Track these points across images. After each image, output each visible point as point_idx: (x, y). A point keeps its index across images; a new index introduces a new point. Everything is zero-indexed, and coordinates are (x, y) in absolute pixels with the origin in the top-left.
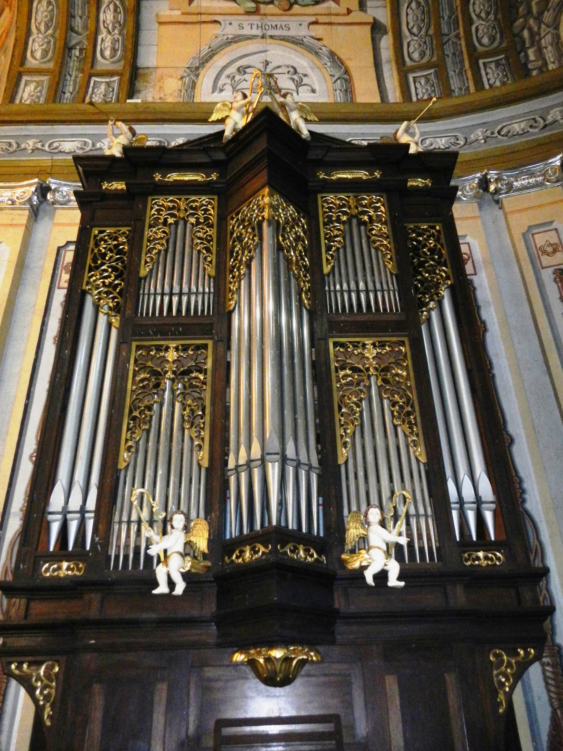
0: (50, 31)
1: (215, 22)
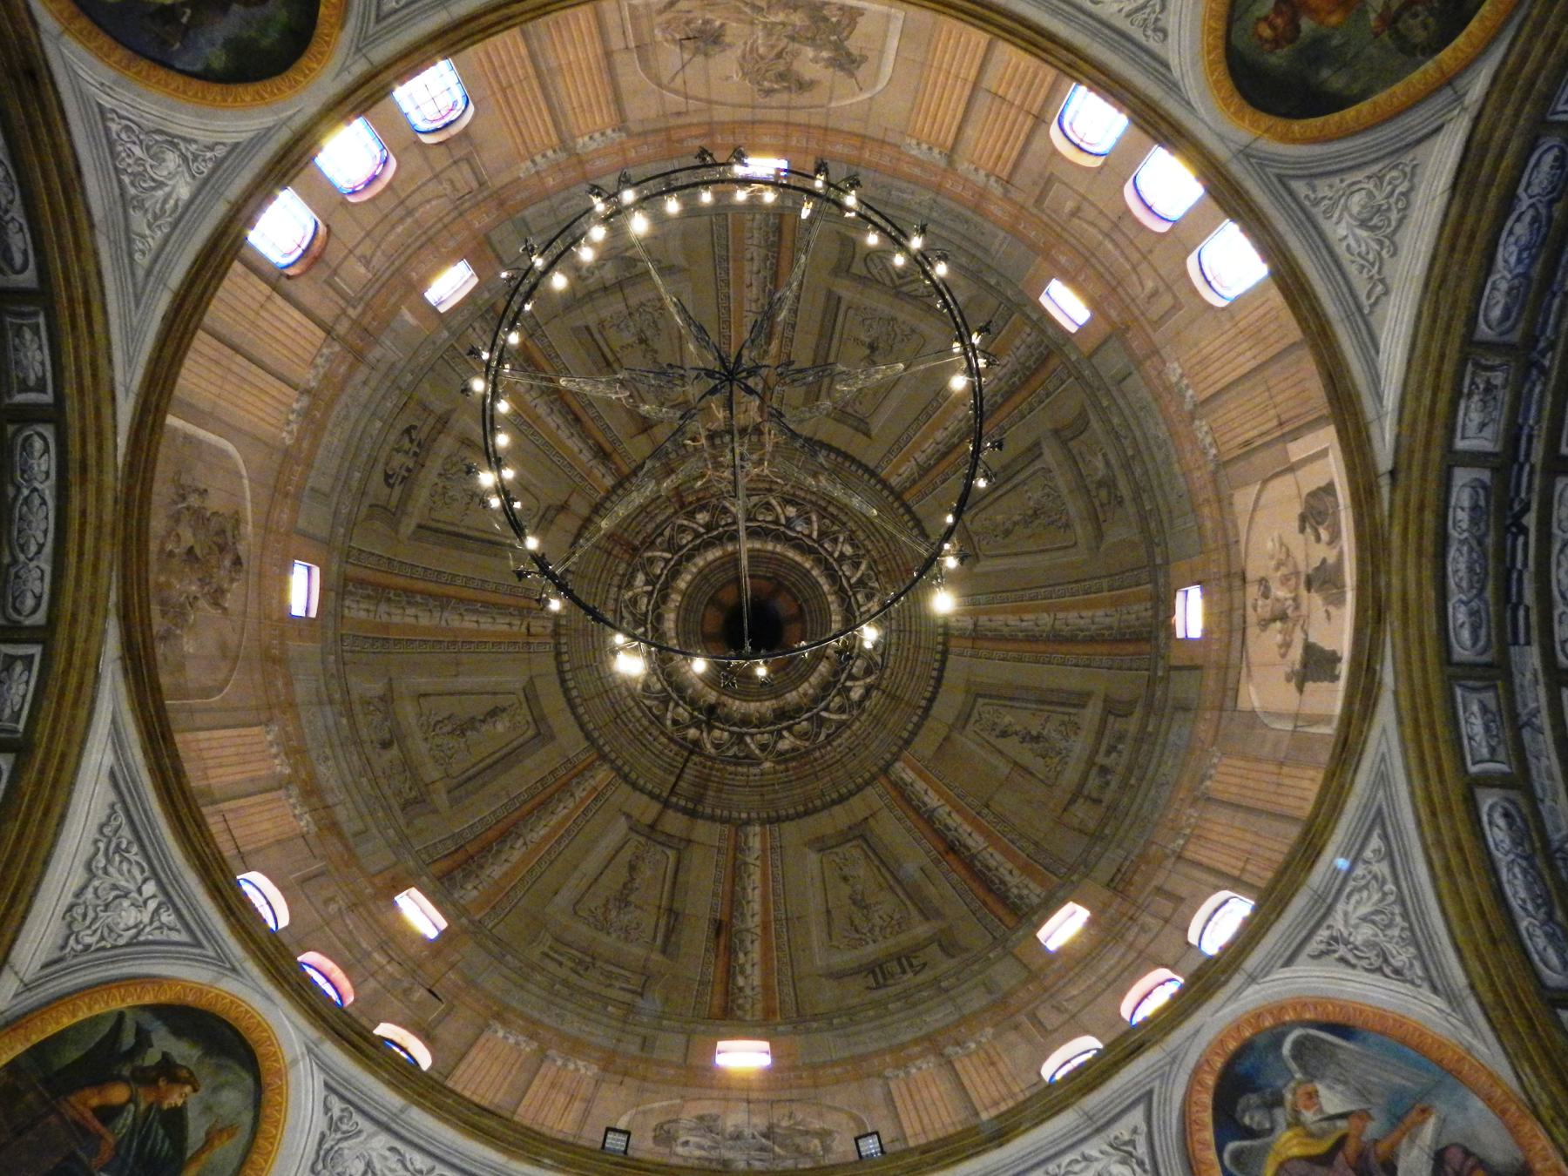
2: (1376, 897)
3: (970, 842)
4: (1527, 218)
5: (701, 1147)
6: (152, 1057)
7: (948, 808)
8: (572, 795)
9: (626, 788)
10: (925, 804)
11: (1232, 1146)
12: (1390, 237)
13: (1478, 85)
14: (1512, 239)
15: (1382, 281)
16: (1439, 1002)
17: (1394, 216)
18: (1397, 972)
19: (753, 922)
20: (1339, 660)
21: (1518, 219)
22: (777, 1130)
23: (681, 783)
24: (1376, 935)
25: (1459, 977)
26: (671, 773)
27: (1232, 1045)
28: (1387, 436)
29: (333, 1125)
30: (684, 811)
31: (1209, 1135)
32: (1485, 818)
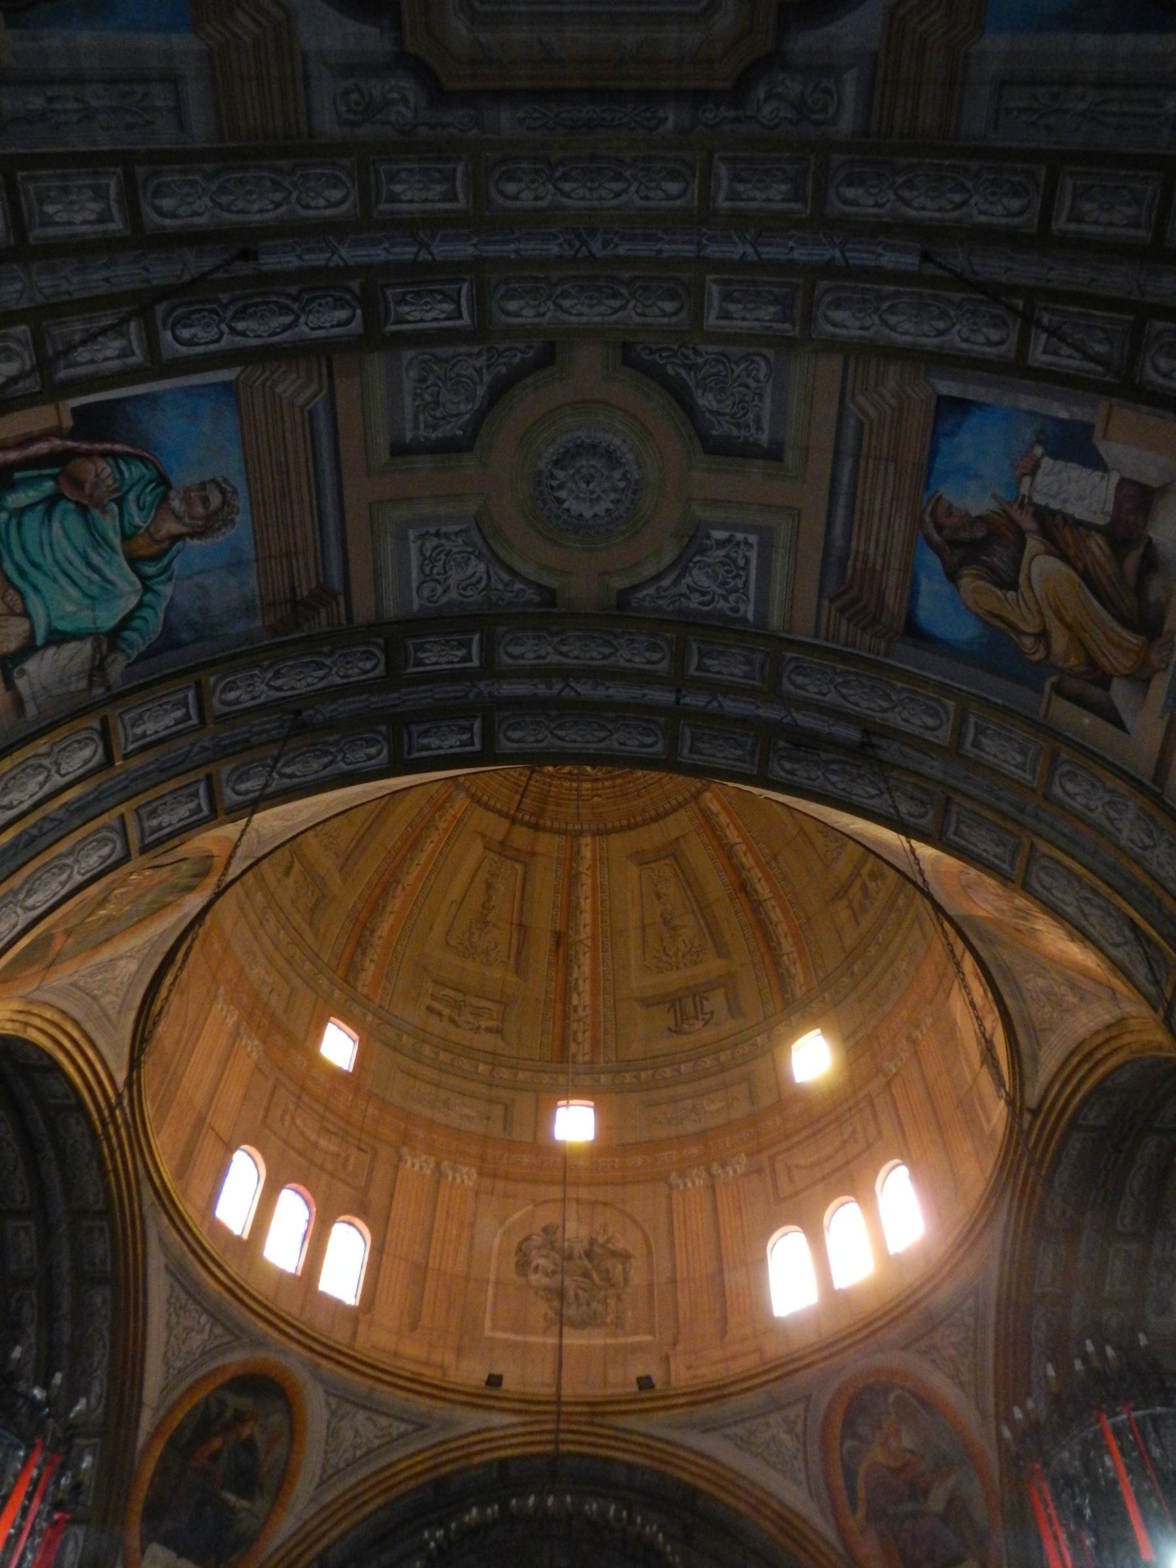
3: (758, 887)
5: (547, 1275)
6: (229, 1413)
7: (744, 848)
8: (437, 829)
9: (479, 811)
10: (726, 836)
11: (848, 1443)
19: (585, 933)
22: (595, 1248)
23: (525, 800)
26: (516, 792)
29: (333, 1413)
30: (528, 825)
31: (837, 1431)
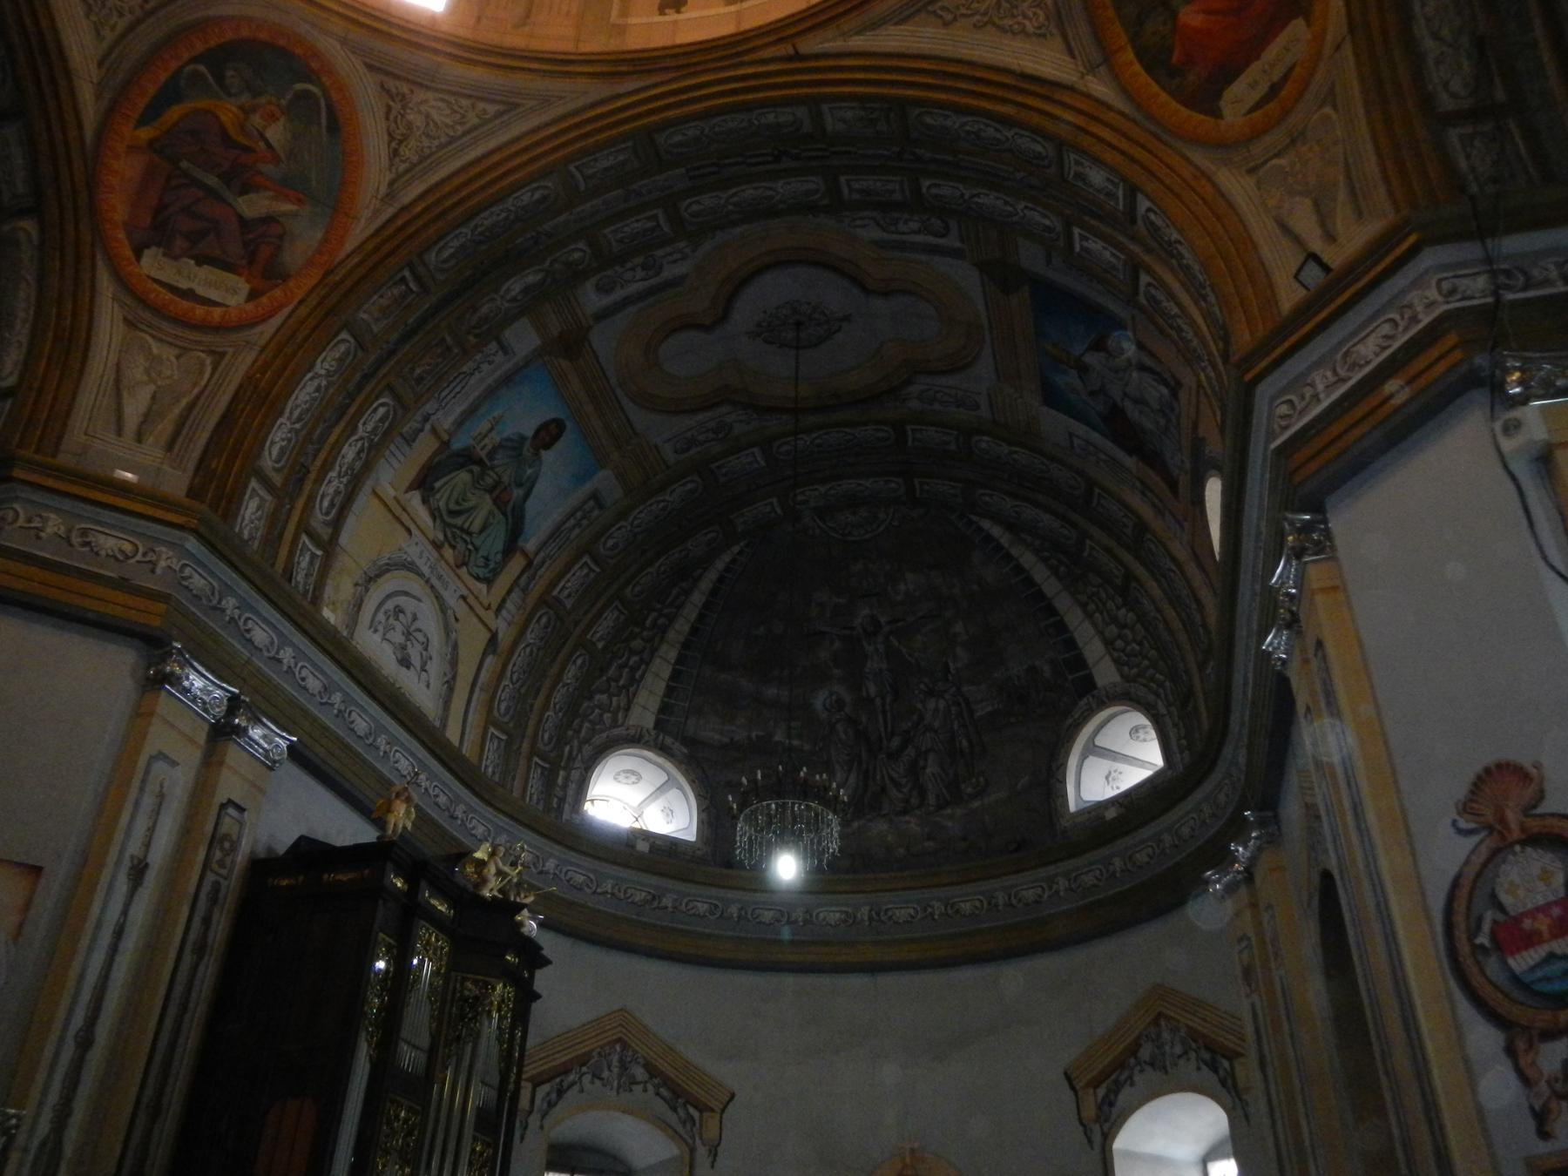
0: (297, 426)
1: (409, 531)
2: (448, 121)
4: (998, 136)
11: (202, 68)
12: (991, 22)
13: (1100, 88)
14: (982, 127)
15: (955, 19)
16: (383, 189)
17: (1008, 22)
18: (396, 153)
20: (678, 12)
21: (997, 130)
24: (418, 128)
25: (407, 199)
27: (282, 42)
28: (826, 45)
31: (200, 47)
32: (535, 185)
